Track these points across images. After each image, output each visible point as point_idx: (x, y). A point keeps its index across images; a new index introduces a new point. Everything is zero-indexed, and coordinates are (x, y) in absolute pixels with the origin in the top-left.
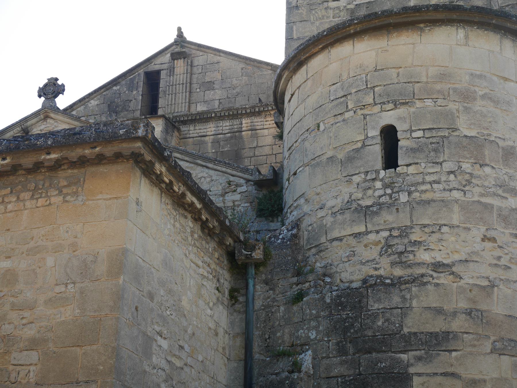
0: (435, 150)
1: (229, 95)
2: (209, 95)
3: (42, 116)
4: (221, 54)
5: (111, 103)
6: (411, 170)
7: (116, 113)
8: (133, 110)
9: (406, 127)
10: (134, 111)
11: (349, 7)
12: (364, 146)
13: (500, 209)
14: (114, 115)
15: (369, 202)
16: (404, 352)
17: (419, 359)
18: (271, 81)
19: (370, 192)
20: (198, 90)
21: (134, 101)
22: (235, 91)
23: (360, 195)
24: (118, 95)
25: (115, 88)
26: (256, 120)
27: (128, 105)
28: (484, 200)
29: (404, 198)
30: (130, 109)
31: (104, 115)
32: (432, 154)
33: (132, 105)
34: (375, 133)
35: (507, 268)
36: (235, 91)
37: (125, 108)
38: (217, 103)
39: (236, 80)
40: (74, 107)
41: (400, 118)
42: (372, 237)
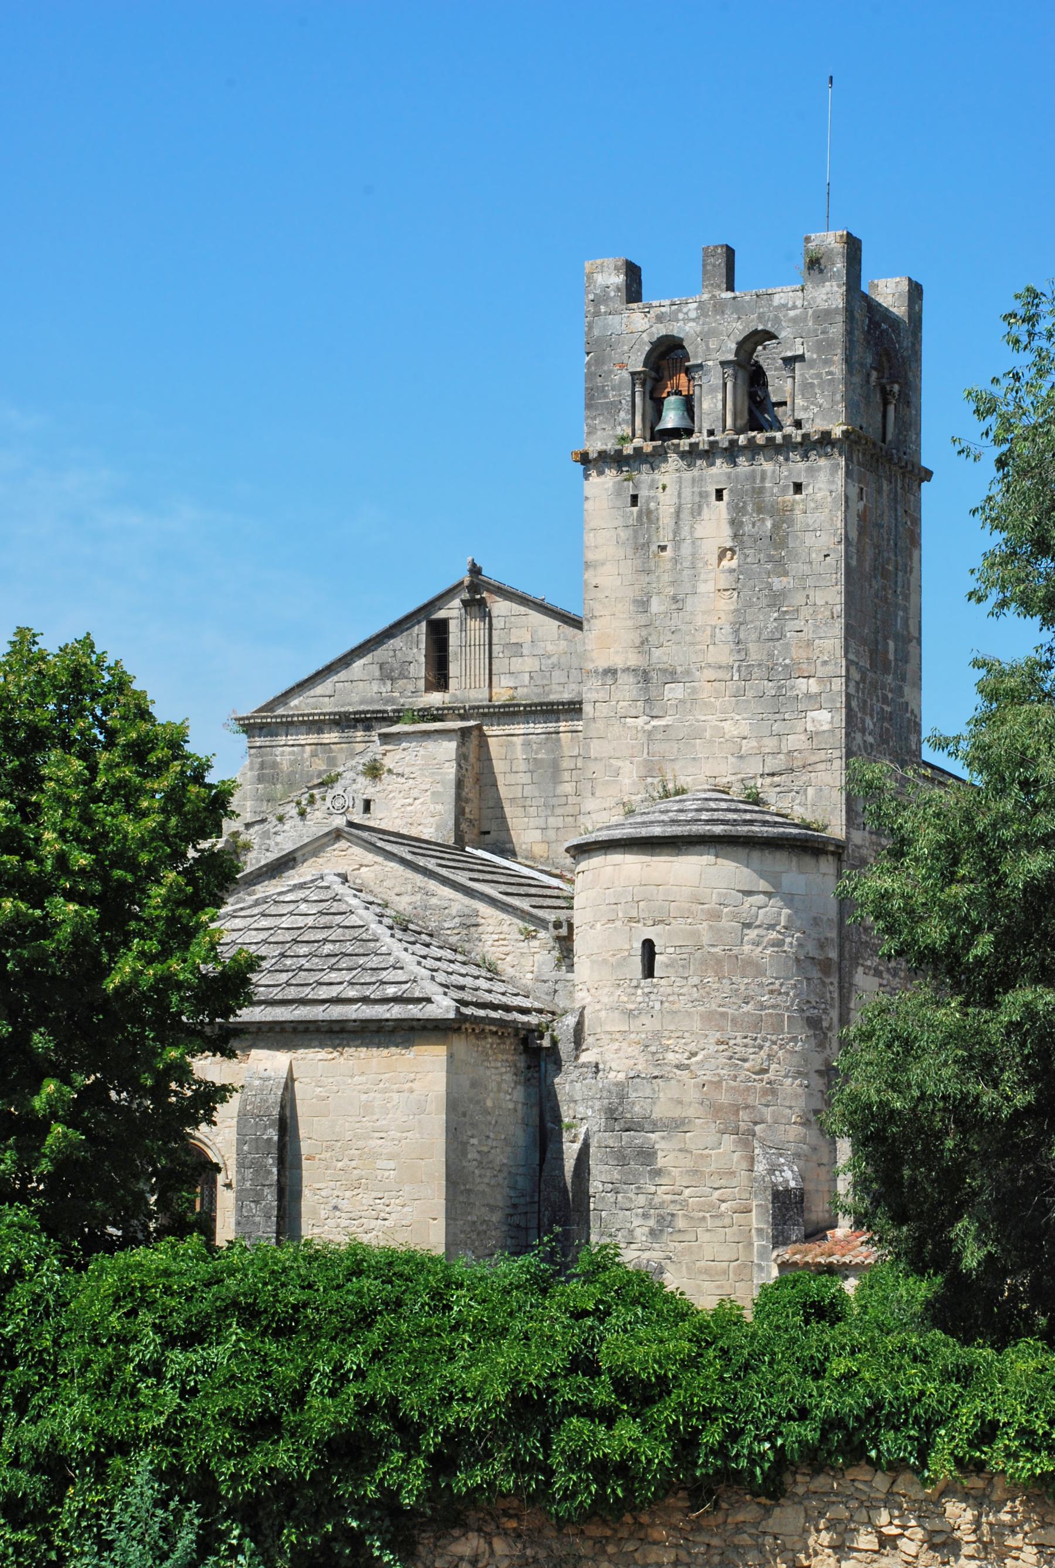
0: (683, 966)
2: (517, 664)
3: (334, 835)
6: (663, 982)
9: (662, 943)
11: (647, 727)
12: (630, 955)
14: (389, 682)
16: (653, 1132)
17: (663, 1138)
19: (633, 997)
20: (501, 655)
22: (550, 662)
23: (626, 999)
24: (391, 653)
29: (657, 1005)
32: (681, 969)
34: (638, 945)
36: (550, 662)
40: (333, 667)
41: (658, 935)
42: (633, 1036)
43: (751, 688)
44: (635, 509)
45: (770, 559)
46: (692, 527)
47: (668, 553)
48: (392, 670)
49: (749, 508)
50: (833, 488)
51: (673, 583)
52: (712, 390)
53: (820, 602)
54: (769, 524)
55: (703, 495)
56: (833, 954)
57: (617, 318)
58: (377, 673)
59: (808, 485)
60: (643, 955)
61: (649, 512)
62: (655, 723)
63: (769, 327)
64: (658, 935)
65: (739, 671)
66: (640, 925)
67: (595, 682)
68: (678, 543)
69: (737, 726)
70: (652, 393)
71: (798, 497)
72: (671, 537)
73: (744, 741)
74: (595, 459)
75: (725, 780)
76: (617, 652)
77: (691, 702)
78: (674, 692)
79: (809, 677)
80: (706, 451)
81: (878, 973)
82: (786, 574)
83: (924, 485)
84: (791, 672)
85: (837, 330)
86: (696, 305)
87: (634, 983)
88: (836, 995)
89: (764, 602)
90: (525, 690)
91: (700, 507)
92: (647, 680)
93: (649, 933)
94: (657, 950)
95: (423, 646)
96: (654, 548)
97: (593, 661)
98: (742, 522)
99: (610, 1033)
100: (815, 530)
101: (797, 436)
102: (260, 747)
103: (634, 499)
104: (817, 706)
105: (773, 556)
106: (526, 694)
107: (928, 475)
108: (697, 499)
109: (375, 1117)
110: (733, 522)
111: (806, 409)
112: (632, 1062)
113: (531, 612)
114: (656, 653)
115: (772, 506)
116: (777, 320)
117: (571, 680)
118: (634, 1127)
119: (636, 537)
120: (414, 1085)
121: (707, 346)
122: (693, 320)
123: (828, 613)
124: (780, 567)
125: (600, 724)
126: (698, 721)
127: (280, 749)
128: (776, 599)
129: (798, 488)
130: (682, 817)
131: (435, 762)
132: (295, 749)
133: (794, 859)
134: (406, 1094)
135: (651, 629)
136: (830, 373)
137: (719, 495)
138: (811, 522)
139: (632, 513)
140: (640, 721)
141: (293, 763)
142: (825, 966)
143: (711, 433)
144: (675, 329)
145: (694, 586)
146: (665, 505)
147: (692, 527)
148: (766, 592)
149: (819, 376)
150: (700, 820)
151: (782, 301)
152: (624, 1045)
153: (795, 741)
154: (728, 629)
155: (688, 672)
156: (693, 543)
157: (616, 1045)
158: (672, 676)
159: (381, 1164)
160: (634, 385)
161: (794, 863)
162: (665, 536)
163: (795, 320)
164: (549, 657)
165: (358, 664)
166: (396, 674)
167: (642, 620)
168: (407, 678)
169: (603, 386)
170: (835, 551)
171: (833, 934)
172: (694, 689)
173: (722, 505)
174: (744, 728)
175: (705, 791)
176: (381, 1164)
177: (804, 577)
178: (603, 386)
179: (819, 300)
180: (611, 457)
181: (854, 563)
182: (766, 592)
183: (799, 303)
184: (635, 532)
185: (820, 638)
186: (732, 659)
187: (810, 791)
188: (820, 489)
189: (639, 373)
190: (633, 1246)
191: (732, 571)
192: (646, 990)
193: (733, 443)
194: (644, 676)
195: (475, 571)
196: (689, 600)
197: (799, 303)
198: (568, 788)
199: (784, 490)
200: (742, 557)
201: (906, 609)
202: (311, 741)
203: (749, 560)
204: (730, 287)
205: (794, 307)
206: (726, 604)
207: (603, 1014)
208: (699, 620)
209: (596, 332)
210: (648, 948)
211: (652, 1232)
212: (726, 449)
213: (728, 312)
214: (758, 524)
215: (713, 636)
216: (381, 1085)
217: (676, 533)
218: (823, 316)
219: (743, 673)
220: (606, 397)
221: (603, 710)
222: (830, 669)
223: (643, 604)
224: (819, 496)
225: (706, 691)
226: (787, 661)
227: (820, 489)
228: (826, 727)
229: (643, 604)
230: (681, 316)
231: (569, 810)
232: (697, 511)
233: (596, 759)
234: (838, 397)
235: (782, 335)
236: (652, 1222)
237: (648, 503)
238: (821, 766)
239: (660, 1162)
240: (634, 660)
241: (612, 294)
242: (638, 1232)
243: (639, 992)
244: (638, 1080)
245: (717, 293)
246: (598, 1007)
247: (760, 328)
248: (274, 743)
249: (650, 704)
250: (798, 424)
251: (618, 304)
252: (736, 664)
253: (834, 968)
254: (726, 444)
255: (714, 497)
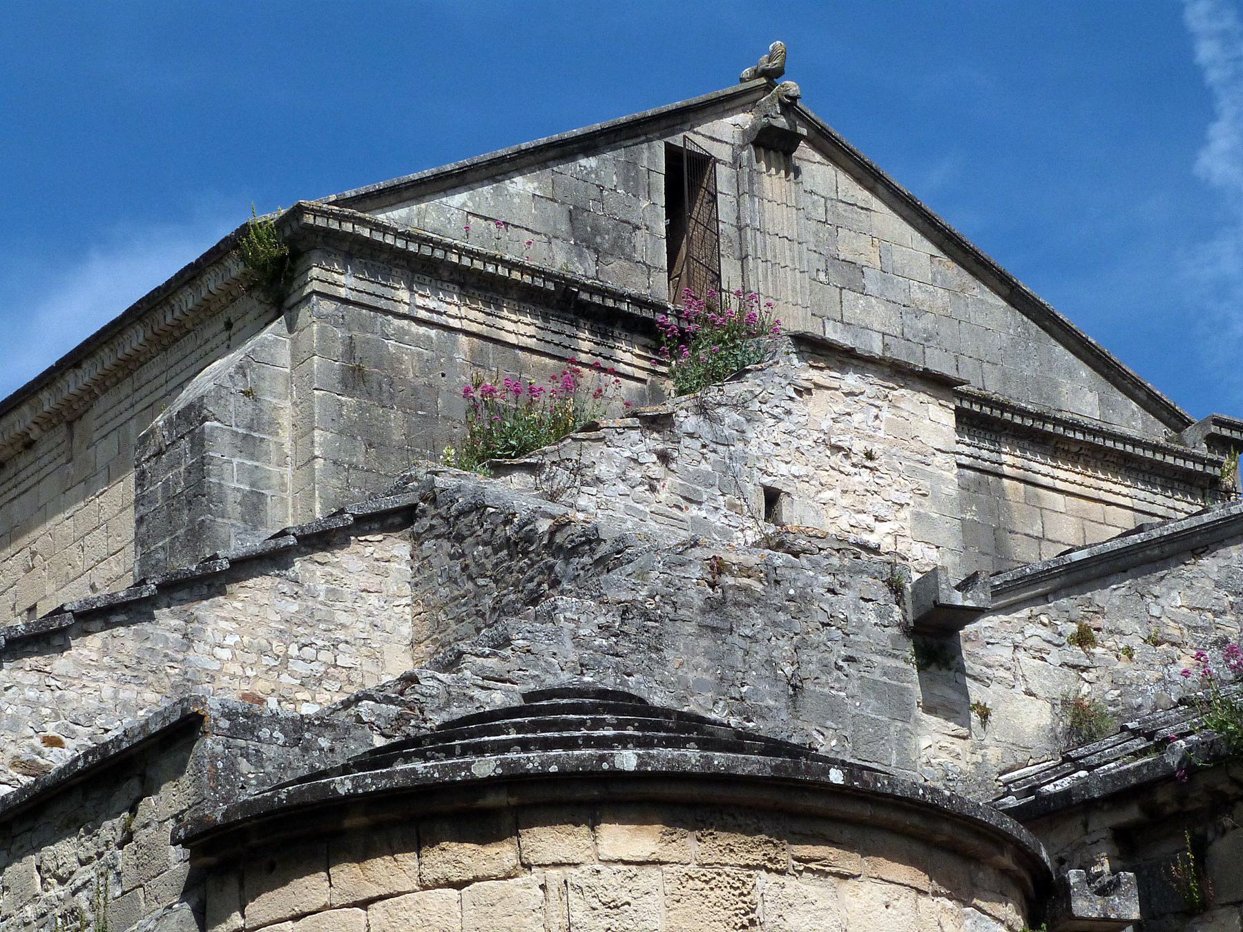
1: (905, 330)
4: (880, 188)
5: (575, 207)
7: (596, 251)
8: (644, 263)
10: (648, 267)
14: (590, 256)
18: (1008, 333)
21: (644, 231)
24: (594, 192)
27: (629, 240)
30: (638, 257)
31: (559, 242)
33: (640, 238)
37: (622, 249)
39: (920, 287)
40: (469, 177)
48: (596, 230)
58: (564, 227)
95: (661, 200)
102: (346, 301)
113: (876, 204)
127: (396, 322)
131: (915, 445)
132: (433, 333)
141: (427, 367)
165: (522, 186)
166: (604, 241)
168: (629, 259)
202: (474, 328)
248: (382, 303)
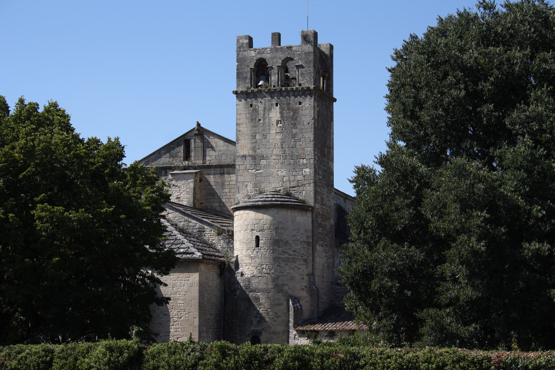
13: (282, 258)
15: (253, 255)
22: (221, 153)
25: (171, 146)
26: (229, 169)
28: (279, 256)
34: (254, 237)
35: (283, 272)
36: (221, 153)
38: (214, 157)
42: (252, 264)
43: (286, 162)
44: (252, 108)
45: (292, 124)
46: (269, 114)
47: (261, 121)
49: (286, 109)
50: (311, 104)
51: (263, 131)
52: (274, 74)
53: (307, 137)
54: (292, 113)
55: (272, 105)
56: (311, 240)
57: (246, 52)
59: (303, 102)
60: (256, 240)
61: (256, 109)
62: (257, 171)
63: (291, 56)
64: (260, 234)
65: (282, 156)
66: (255, 231)
67: (240, 159)
68: (264, 119)
69: (283, 173)
70: (256, 74)
71: (300, 106)
72: (262, 117)
73: (284, 177)
74: (240, 93)
75: (278, 189)
76: (246, 150)
77: (268, 166)
78: (263, 162)
79: (303, 159)
80: (273, 92)
81: (322, 246)
82: (297, 128)
83: (334, 103)
84: (299, 157)
85: (311, 58)
86: (269, 49)
87: (253, 248)
88: (311, 252)
89: (290, 136)
90: (214, 161)
91: (271, 108)
92: (255, 159)
93: (258, 234)
94: (260, 239)
96: (257, 120)
97: (239, 153)
98: (284, 113)
99: (245, 263)
100: (305, 116)
101: (300, 88)
103: (251, 105)
104: (306, 167)
105: (293, 123)
106: (214, 162)
107: (335, 100)
108: (270, 106)
109: (177, 288)
110: (281, 113)
111: (302, 80)
112: (252, 272)
114: (258, 151)
115: (293, 108)
116: (294, 54)
117: (228, 158)
118: (253, 291)
119: (252, 117)
120: (189, 278)
121: (273, 61)
122: (269, 54)
123: (309, 140)
124: (295, 126)
125: (241, 172)
126: (271, 171)
128: (294, 136)
129: (300, 103)
130: (267, 199)
133: (300, 212)
134: (187, 281)
135: (256, 144)
136: (310, 70)
137: (277, 105)
138: (304, 113)
139: (251, 109)
140: (253, 171)
142: (308, 243)
143: (274, 86)
144: (263, 56)
145: (269, 131)
146: (261, 107)
147: (269, 114)
148: (291, 133)
149: (306, 71)
150: (273, 200)
151: (295, 49)
152: (250, 267)
153: (299, 177)
154: (279, 144)
155: (267, 157)
156: (269, 119)
157: (247, 267)
158: (263, 158)
159: (179, 302)
160: (251, 72)
161: (300, 213)
162: (261, 116)
163: (299, 55)
164: (221, 151)
167: (254, 141)
169: (242, 72)
170: (311, 122)
171: (311, 234)
172: (269, 162)
173: (278, 108)
174: (284, 173)
175: (272, 192)
176: (179, 302)
177: (302, 129)
178: (242, 72)
179: (306, 49)
180: (244, 93)
181: (316, 125)
182: (291, 133)
183: (300, 50)
184: (252, 115)
185: (307, 147)
186: (281, 153)
187: (304, 192)
188: (307, 104)
189: (253, 68)
190: (253, 326)
191: (280, 127)
192: (257, 251)
193: (281, 90)
194: (254, 158)
195: (198, 125)
196: (268, 136)
197: (300, 50)
198: (227, 190)
199: (296, 104)
200: (284, 123)
201: (330, 139)
203: (286, 124)
204: (280, 45)
205: (299, 51)
206: (279, 137)
207: (244, 258)
208: (271, 141)
209: (240, 56)
210: (257, 238)
211: (258, 321)
212: (279, 91)
213: (279, 52)
214: (288, 113)
215: (275, 146)
216: (179, 278)
217: (264, 115)
218: (307, 54)
219: (284, 157)
220: (243, 75)
221: (242, 167)
222: (310, 157)
223: (254, 137)
224: (306, 106)
225: (272, 162)
226: (297, 154)
227: (307, 104)
228: (308, 174)
229: (254, 137)
230: (265, 52)
231: (227, 197)
232: (270, 109)
233: (240, 182)
234: (312, 77)
235: (295, 59)
236: (258, 319)
237: (255, 106)
238: (307, 185)
239: (261, 301)
240: (251, 153)
241: (245, 45)
242: (254, 322)
243: (255, 251)
244: (254, 277)
245: (276, 46)
246: (242, 256)
247: (289, 56)
249: (256, 166)
250: (300, 85)
251: (246, 49)
252: (282, 155)
253: (311, 244)
254: (279, 90)
255: (275, 105)
